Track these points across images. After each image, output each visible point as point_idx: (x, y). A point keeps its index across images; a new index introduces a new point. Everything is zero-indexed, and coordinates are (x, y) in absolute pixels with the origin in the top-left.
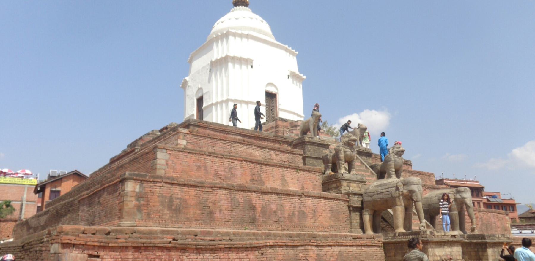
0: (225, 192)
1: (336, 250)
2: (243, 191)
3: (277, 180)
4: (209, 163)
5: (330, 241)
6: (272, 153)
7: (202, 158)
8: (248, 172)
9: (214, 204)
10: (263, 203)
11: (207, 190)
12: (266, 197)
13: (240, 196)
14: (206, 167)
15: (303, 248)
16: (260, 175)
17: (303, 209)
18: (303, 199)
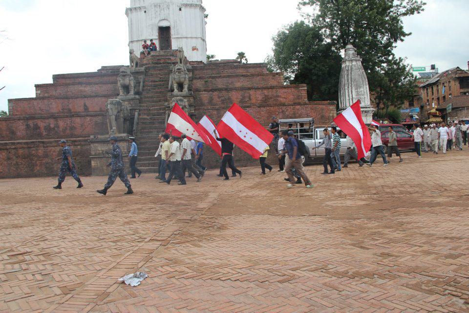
13: (31, 123)
14: (34, 106)
18: (74, 119)
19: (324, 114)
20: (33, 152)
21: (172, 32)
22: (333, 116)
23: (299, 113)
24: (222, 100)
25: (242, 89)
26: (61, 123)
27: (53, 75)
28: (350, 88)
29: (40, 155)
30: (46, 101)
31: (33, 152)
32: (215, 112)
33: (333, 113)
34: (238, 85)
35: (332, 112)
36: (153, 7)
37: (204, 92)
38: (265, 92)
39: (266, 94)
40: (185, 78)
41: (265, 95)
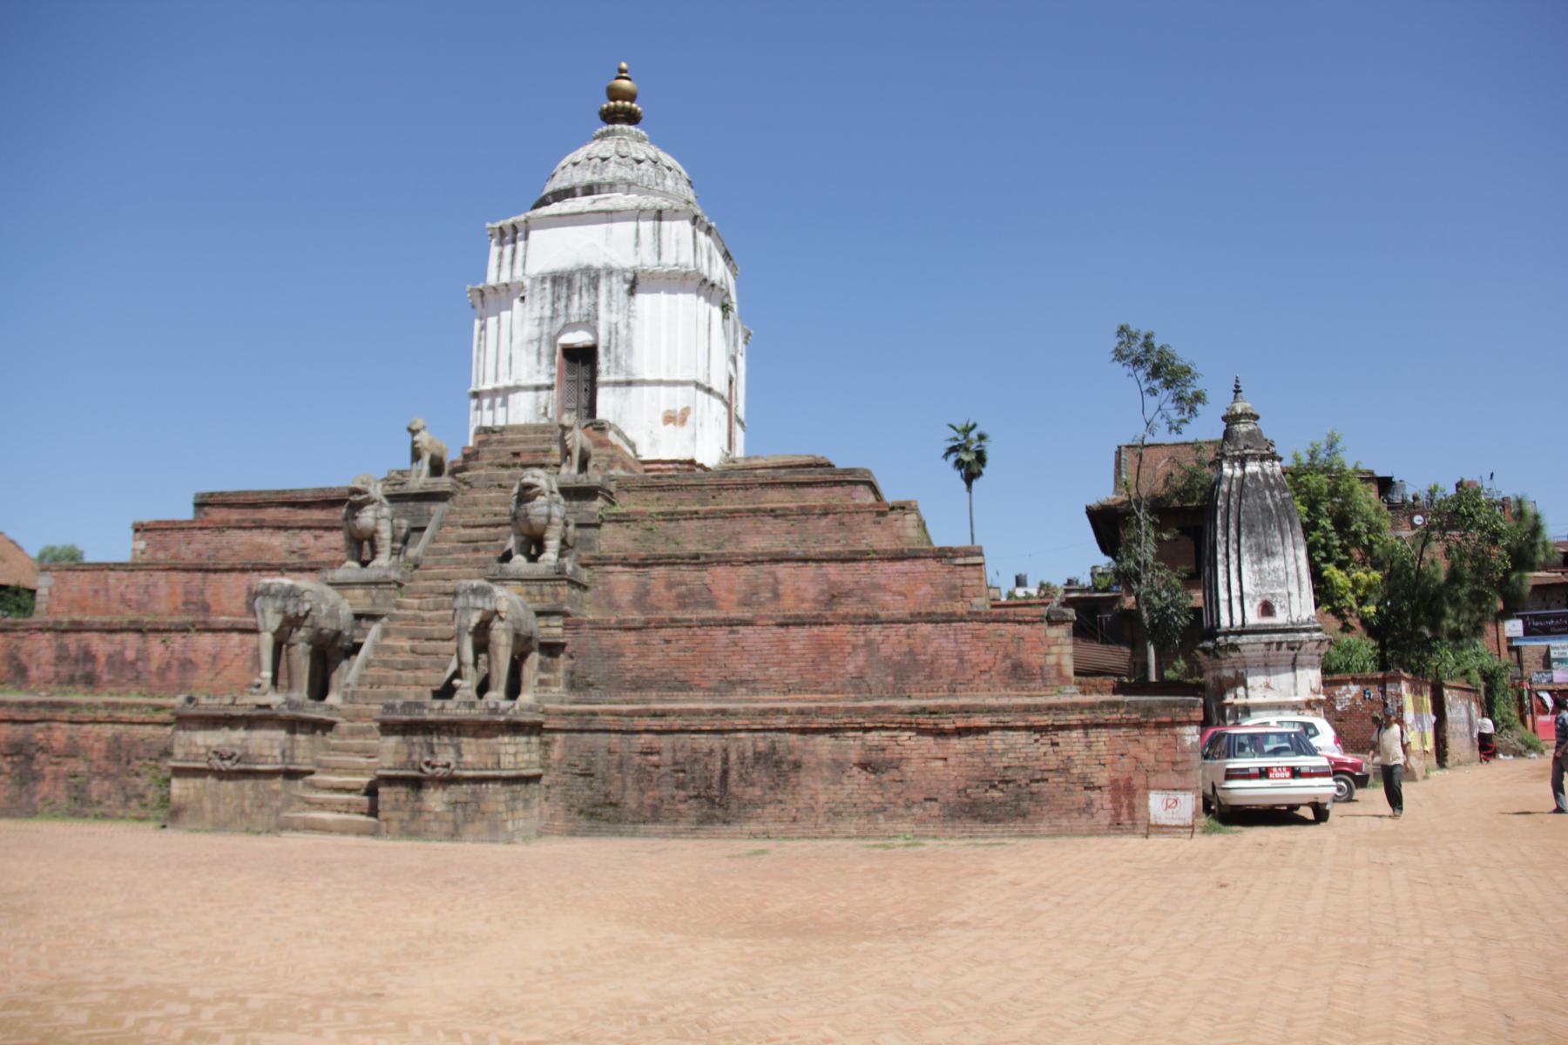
0: (48, 635)
1: (109, 731)
2: (78, 631)
3: (236, 597)
4: (112, 581)
5: (102, 714)
6: (307, 536)
7: (102, 575)
8: (180, 590)
9: (30, 655)
10: (110, 649)
11: (20, 634)
12: (117, 637)
13: (72, 640)
14: (107, 590)
15: (43, 725)
16: (202, 592)
17: (191, 655)
19: (1023, 656)
20: (40, 736)
21: (603, 362)
22: (1059, 665)
23: (930, 649)
24: (679, 596)
25: (753, 560)
26: (155, 644)
27: (197, 496)
28: (1233, 557)
29: (55, 744)
30: (141, 577)
31: (40, 736)
32: (631, 637)
33: (1059, 655)
34: (756, 543)
35: (1055, 649)
36: (548, 285)
37: (619, 568)
38: (832, 570)
39: (834, 578)
40: (549, 516)
41: (832, 585)
